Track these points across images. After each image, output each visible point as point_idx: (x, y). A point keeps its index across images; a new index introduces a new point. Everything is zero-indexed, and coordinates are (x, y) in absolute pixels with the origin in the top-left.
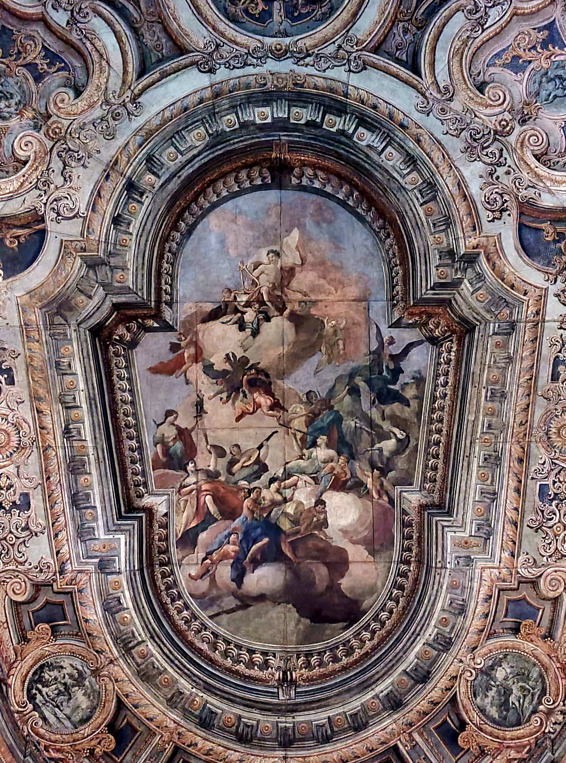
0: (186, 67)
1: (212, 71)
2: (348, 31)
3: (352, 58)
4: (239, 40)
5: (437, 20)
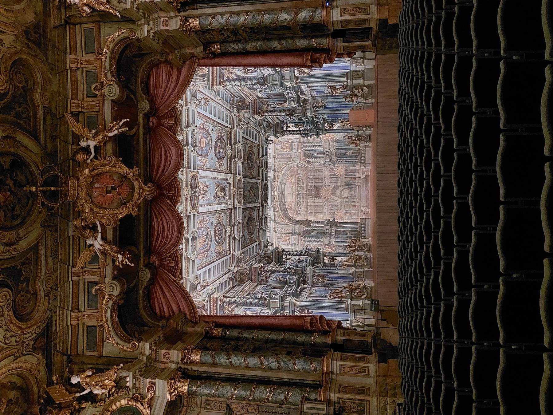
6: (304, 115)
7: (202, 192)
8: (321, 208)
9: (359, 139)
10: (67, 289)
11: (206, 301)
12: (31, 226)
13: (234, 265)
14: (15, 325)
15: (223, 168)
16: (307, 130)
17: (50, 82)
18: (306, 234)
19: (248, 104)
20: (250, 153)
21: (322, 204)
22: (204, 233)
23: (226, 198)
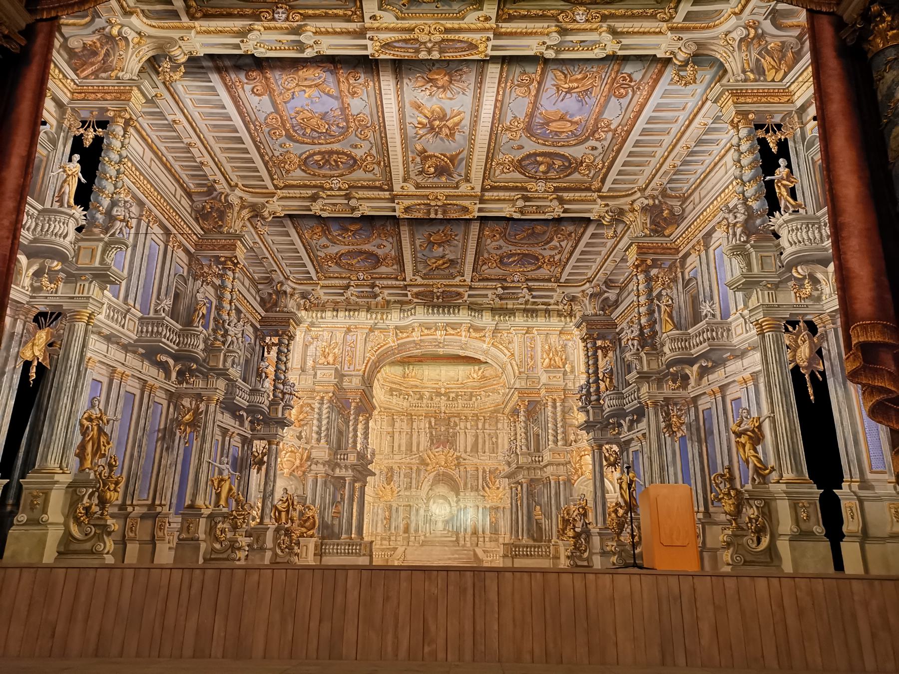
6: (644, 377)
7: (437, 123)
8: (403, 448)
9: (577, 536)
11: (120, 74)
13: (246, 196)
15: (498, 172)
16: (598, 400)
18: (340, 403)
19: (667, 232)
20: (537, 259)
21: (414, 449)
22: (334, 128)
23: (419, 179)
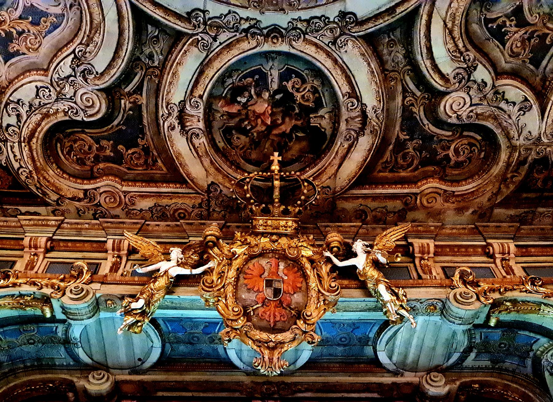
0: (368, 20)
1: (343, 15)
2: (207, 56)
3: (202, 27)
4: (313, 48)
5: (121, 64)
10: (93, 232)
12: (211, 162)
14: (38, 125)
17: (460, 210)
